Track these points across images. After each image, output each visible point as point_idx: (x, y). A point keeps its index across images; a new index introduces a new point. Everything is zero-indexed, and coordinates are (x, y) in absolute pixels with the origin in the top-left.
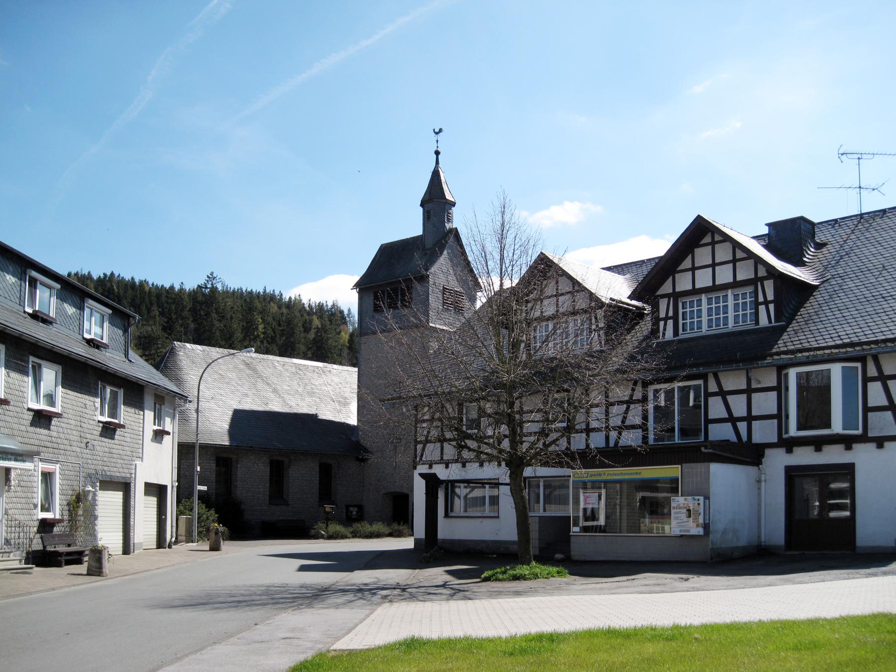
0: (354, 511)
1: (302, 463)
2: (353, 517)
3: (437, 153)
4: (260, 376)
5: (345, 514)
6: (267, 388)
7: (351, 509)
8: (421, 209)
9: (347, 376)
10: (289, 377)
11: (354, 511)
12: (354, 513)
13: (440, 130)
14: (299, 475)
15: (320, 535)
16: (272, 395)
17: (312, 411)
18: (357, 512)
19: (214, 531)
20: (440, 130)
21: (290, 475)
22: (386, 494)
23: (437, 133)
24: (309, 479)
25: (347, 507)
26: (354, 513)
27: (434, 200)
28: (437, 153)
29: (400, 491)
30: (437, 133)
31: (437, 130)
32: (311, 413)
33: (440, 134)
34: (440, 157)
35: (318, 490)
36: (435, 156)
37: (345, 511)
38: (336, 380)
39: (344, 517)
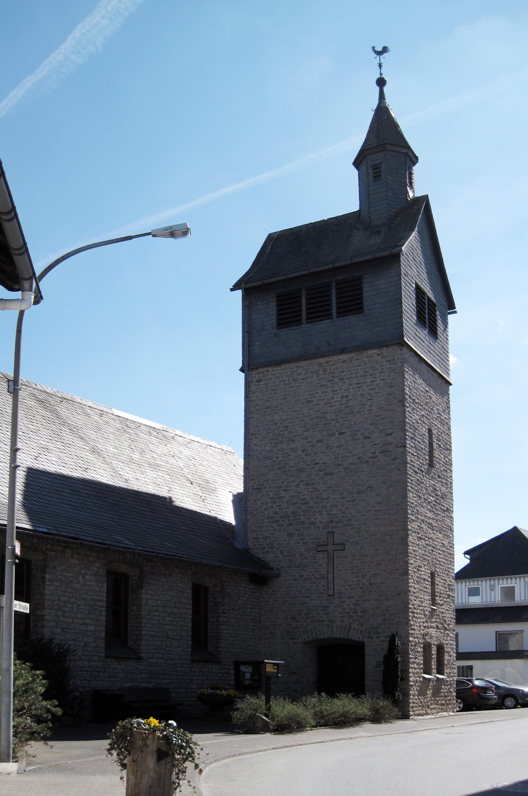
0: (247, 670)
1: (164, 580)
2: (247, 682)
3: (381, 82)
4: (64, 424)
5: (233, 677)
6: (81, 444)
7: (243, 668)
8: (355, 172)
9: (200, 449)
10: (112, 434)
11: (247, 670)
12: (248, 676)
13: (385, 50)
14: (159, 603)
15: (259, 724)
16: (92, 457)
17: (163, 492)
18: (252, 674)
19: (152, 745)
20: (385, 50)
21: (144, 602)
22: (306, 643)
23: (379, 53)
24: (176, 611)
25: (237, 664)
26: (248, 676)
27: (388, 146)
28: (381, 82)
29: (345, 636)
30: (379, 53)
31: (379, 49)
32: (161, 495)
33: (385, 55)
34: (385, 89)
35: (190, 634)
36: (377, 89)
37: (232, 672)
38: (186, 452)
39: (232, 683)
